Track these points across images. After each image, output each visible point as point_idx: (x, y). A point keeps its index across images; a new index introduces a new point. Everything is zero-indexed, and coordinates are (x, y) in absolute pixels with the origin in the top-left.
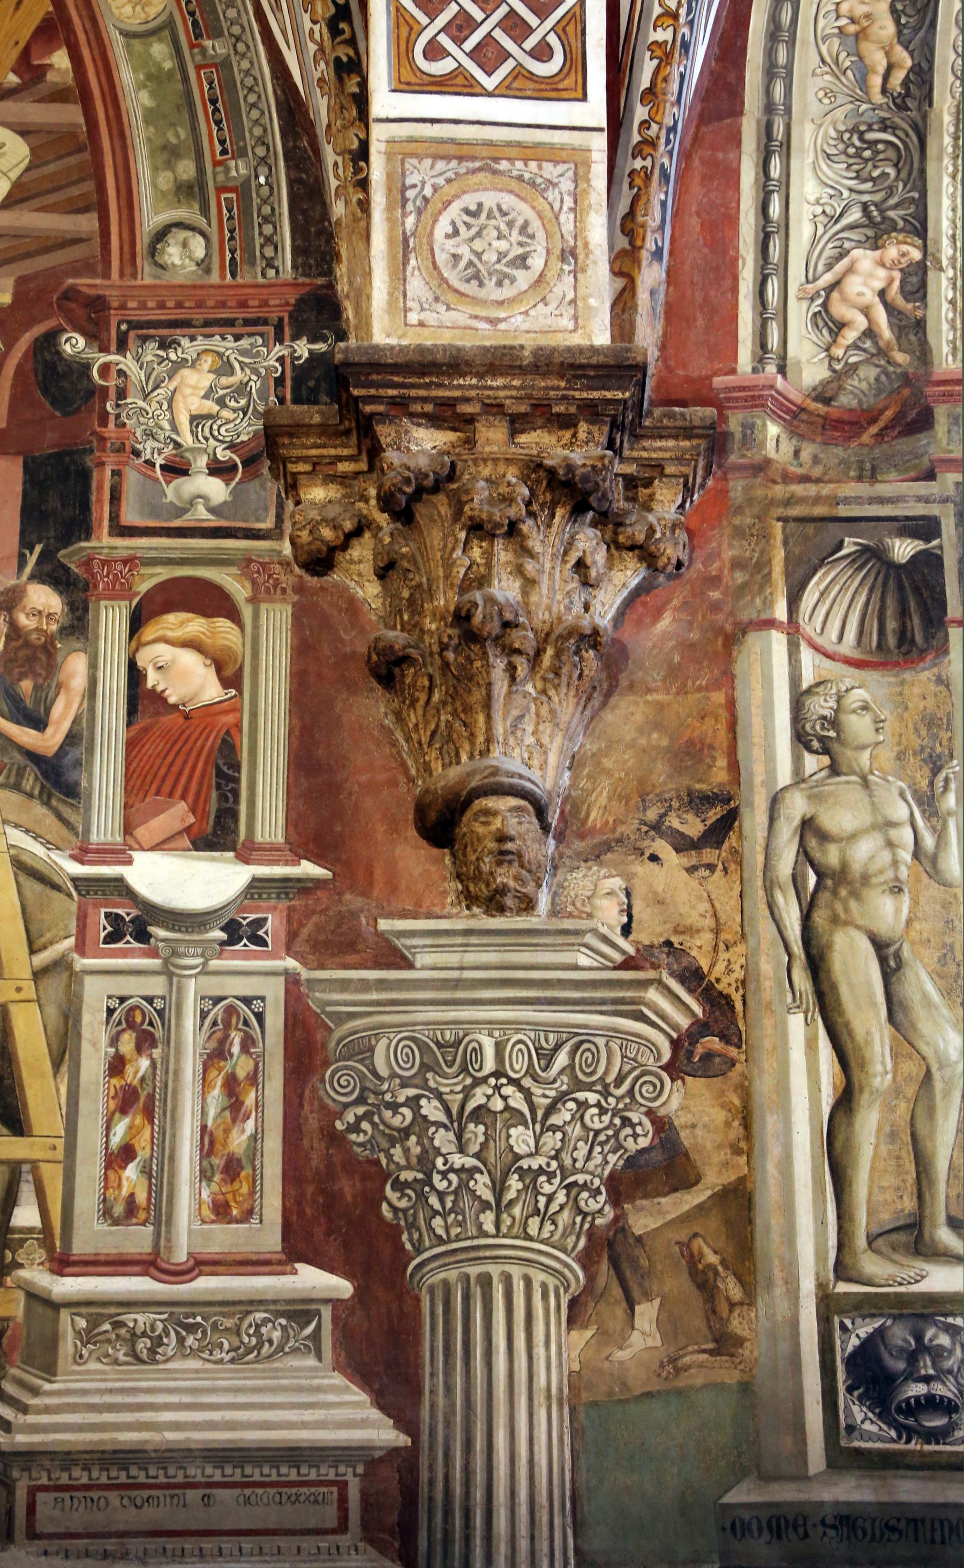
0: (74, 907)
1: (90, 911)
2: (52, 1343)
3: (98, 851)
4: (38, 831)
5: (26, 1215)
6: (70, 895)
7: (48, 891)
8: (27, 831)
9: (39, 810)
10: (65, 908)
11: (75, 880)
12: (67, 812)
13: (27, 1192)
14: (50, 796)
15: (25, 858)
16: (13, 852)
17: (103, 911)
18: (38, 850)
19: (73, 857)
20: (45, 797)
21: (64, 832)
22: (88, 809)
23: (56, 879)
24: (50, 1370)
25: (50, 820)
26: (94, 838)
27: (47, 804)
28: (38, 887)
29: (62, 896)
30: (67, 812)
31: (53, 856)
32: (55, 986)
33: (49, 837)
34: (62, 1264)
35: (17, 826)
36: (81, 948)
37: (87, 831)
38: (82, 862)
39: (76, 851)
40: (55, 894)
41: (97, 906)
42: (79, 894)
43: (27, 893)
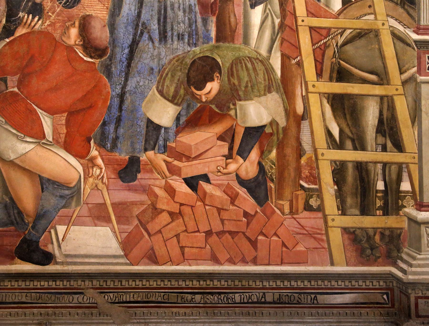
0: (416, 54)
1: (422, 56)
2: (419, 238)
3: (424, 29)
4: (400, 19)
5: (405, 186)
6: (414, 49)
7: (406, 46)
8: (396, 20)
9: (401, 10)
10: (412, 54)
11: (415, 42)
12: (411, 11)
13: (405, 176)
14: (404, 4)
15: (396, 32)
16: (391, 29)
17: (427, 55)
18: (400, 28)
19: (414, 32)
20: (402, 5)
21: (411, 21)
22: (419, 10)
23: (409, 42)
24: (419, 250)
25: (405, 15)
26: (422, 23)
27: (403, 7)
28: (402, 45)
29: (411, 49)
30: (411, 11)
31: (407, 31)
32: (410, 87)
33: (405, 22)
34: (421, 206)
35: (392, 17)
36: (419, 72)
37: (419, 20)
38: (418, 34)
39: (415, 29)
40: (408, 48)
41: (425, 53)
42: (418, 48)
43: (398, 48)
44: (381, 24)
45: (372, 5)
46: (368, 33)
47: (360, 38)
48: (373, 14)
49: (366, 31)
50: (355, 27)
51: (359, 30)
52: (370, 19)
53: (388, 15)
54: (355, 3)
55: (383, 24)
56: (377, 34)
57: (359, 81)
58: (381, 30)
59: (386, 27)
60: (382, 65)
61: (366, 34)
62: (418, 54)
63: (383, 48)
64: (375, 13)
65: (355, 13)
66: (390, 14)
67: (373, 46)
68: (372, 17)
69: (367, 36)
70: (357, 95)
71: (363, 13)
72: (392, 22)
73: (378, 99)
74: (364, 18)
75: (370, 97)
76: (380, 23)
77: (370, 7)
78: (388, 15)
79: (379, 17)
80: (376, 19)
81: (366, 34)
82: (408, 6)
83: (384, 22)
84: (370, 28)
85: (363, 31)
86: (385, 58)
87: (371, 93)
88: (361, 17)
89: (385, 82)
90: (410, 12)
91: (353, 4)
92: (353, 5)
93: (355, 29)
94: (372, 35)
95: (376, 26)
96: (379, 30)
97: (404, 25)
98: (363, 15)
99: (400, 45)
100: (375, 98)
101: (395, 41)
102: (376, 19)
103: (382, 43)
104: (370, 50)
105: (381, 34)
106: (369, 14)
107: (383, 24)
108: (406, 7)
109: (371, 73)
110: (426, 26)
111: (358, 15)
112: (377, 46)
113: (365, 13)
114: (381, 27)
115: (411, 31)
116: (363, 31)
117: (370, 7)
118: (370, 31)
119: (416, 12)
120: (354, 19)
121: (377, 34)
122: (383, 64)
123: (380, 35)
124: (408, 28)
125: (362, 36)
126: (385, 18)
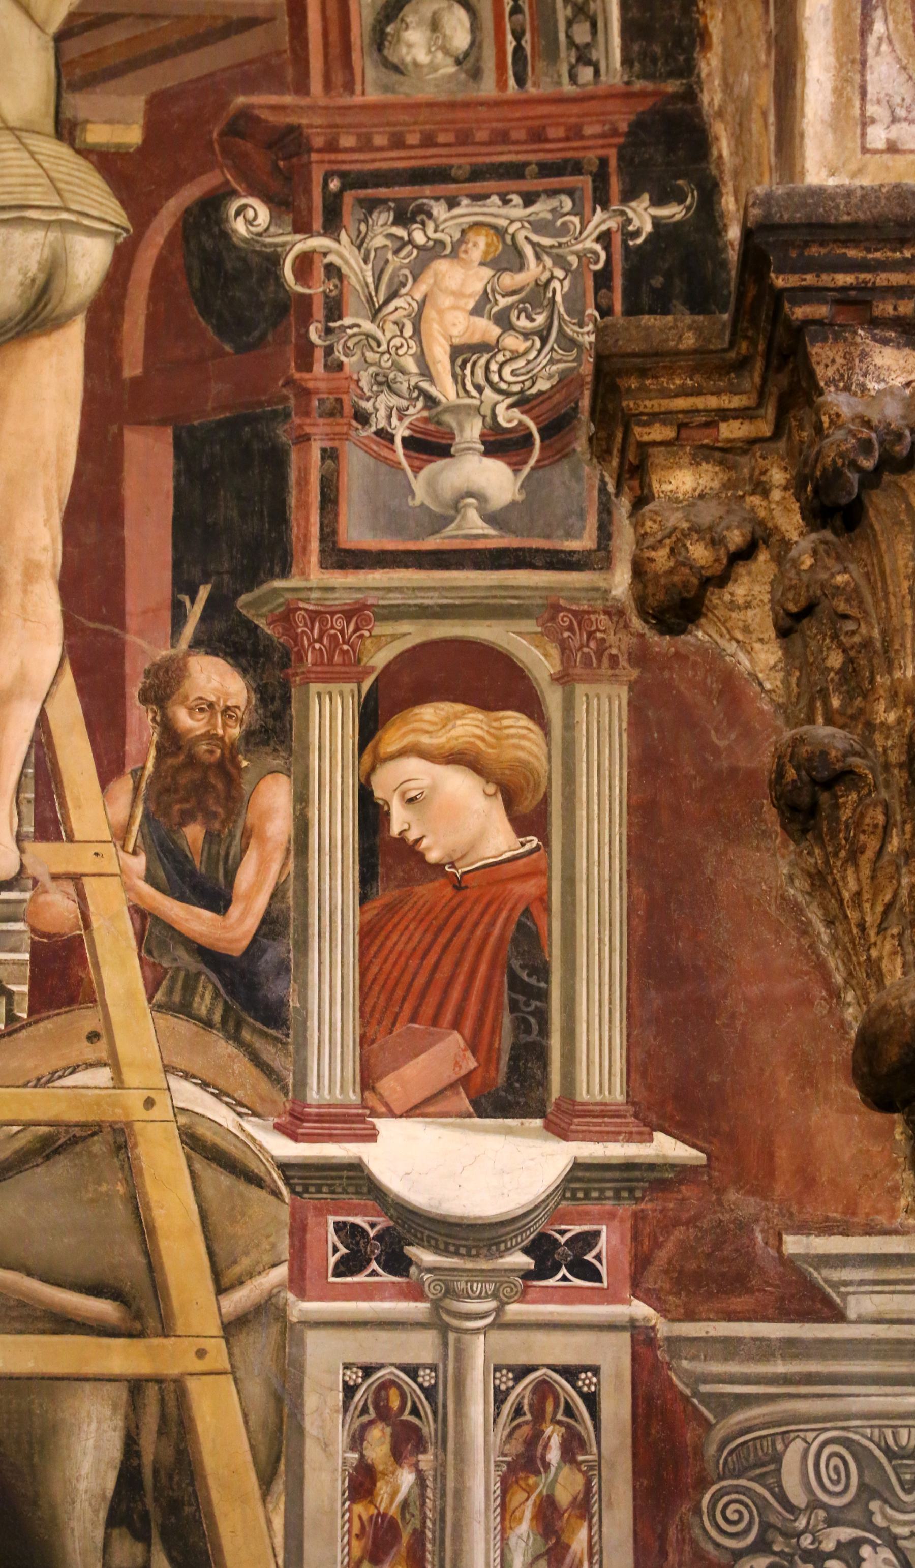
0: (284, 1213)
1: (311, 1220)
3: (320, 1118)
4: (222, 1084)
6: (276, 1194)
7: (242, 1186)
8: (205, 1085)
9: (224, 1048)
11: (284, 1167)
14: (239, 1025)
15: (202, 1130)
16: (182, 1120)
17: (331, 1219)
20: (231, 1025)
21: (265, 1086)
22: (302, 1044)
23: (254, 1166)
25: (241, 1065)
27: (235, 1038)
28: (225, 1180)
29: (263, 1194)
30: (268, 1052)
31: (247, 1127)
33: (239, 1094)
35: (187, 1076)
37: (301, 1083)
38: (295, 1137)
39: (285, 1119)
40: (254, 1193)
41: (321, 1212)
42: (293, 1191)
43: (209, 1191)
44: (140, 1104)
45: (103, 1032)
46: (84, 1139)
47: (48, 1158)
48: (105, 1065)
49: (77, 1131)
50: (28, 1115)
51: (45, 1129)
52: (91, 1083)
53: (168, 1069)
54: (29, 1025)
55: (149, 1103)
56: (121, 1140)
57: (40, 1325)
58: (137, 1126)
59: (162, 1110)
60: (142, 1260)
61: (74, 1141)
62: (293, 1215)
63: (145, 1194)
64: (114, 1062)
65: (30, 1064)
66: (179, 1061)
67: (104, 1188)
68: (103, 1076)
69: (78, 1148)
70: (30, 1378)
71: (63, 1063)
72: (188, 1095)
73: (121, 1393)
74: (69, 1081)
75: (88, 1386)
76: (134, 1100)
77: (93, 1037)
78: (168, 1069)
79: (130, 1077)
80: (118, 1082)
81: (74, 1141)
82: (254, 1030)
83: (152, 1094)
84: (91, 1118)
85: (62, 1129)
86: (152, 1232)
87: (92, 1369)
88: (54, 1076)
89: (152, 1323)
90: (265, 1057)
91: (23, 1027)
92: (23, 1034)
93: (27, 1125)
94: (98, 1146)
95: (119, 1111)
96: (129, 1124)
97: (238, 1105)
98: (65, 1069)
99: (217, 1181)
100: (108, 1386)
101: (198, 1166)
102: (118, 1082)
103: (141, 1174)
104: (92, 1201)
105: (140, 1139)
106: (89, 1065)
107: (149, 1103)
108: (246, 1035)
109: (95, 1290)
110: (330, 1106)
111: (44, 1071)
112: (121, 1188)
113: (73, 1061)
114: (138, 1112)
115: (264, 1128)
116: (62, 1129)
117: (93, 1037)
118: (93, 1129)
119: (287, 1054)
120: (25, 1085)
121: (122, 1140)
122: (147, 1254)
123: (135, 1145)
124: (255, 1114)
125: (57, 1151)
126: (158, 1079)
